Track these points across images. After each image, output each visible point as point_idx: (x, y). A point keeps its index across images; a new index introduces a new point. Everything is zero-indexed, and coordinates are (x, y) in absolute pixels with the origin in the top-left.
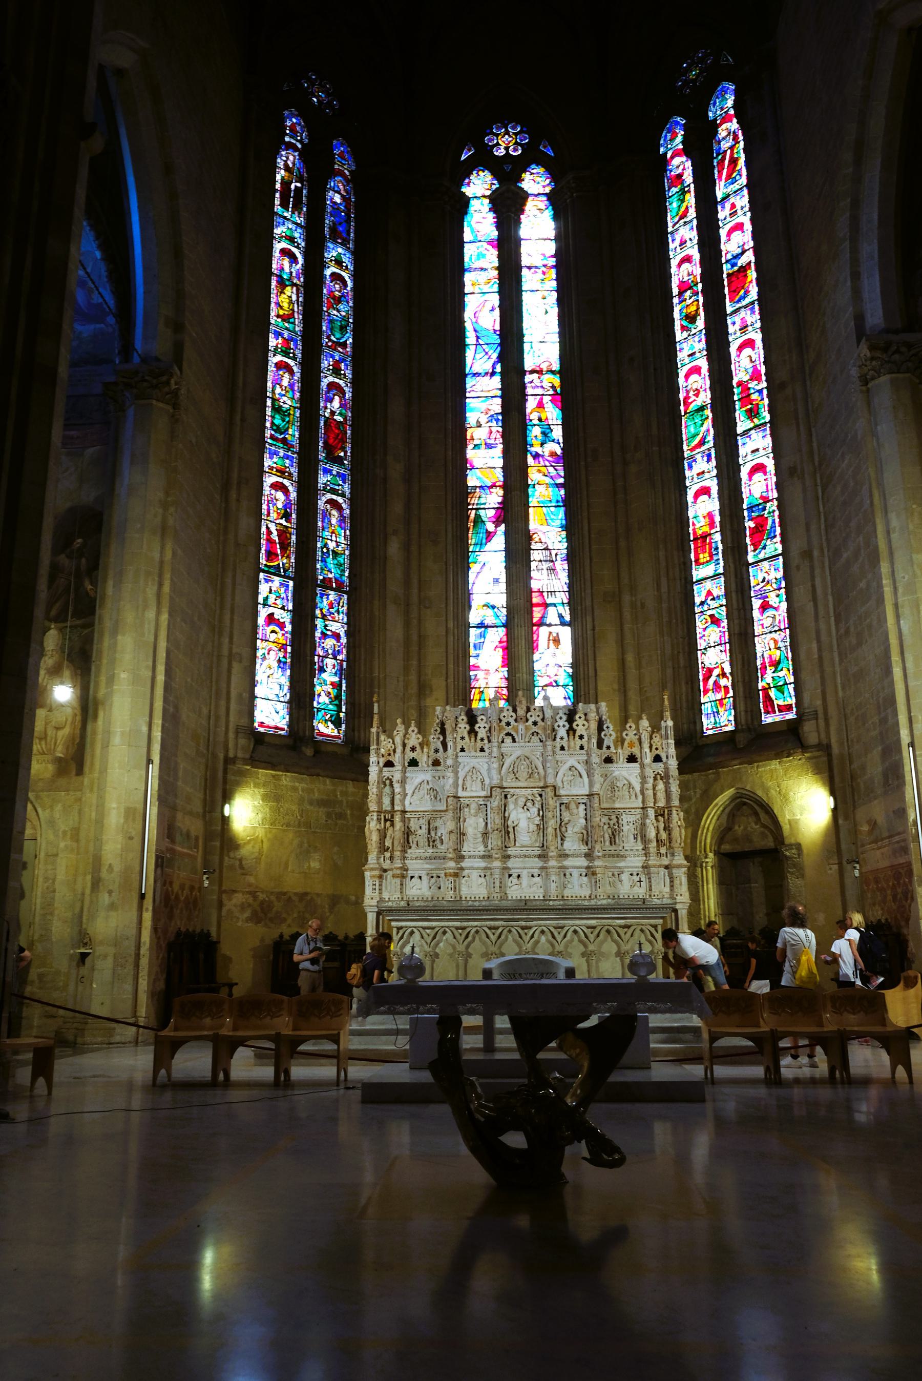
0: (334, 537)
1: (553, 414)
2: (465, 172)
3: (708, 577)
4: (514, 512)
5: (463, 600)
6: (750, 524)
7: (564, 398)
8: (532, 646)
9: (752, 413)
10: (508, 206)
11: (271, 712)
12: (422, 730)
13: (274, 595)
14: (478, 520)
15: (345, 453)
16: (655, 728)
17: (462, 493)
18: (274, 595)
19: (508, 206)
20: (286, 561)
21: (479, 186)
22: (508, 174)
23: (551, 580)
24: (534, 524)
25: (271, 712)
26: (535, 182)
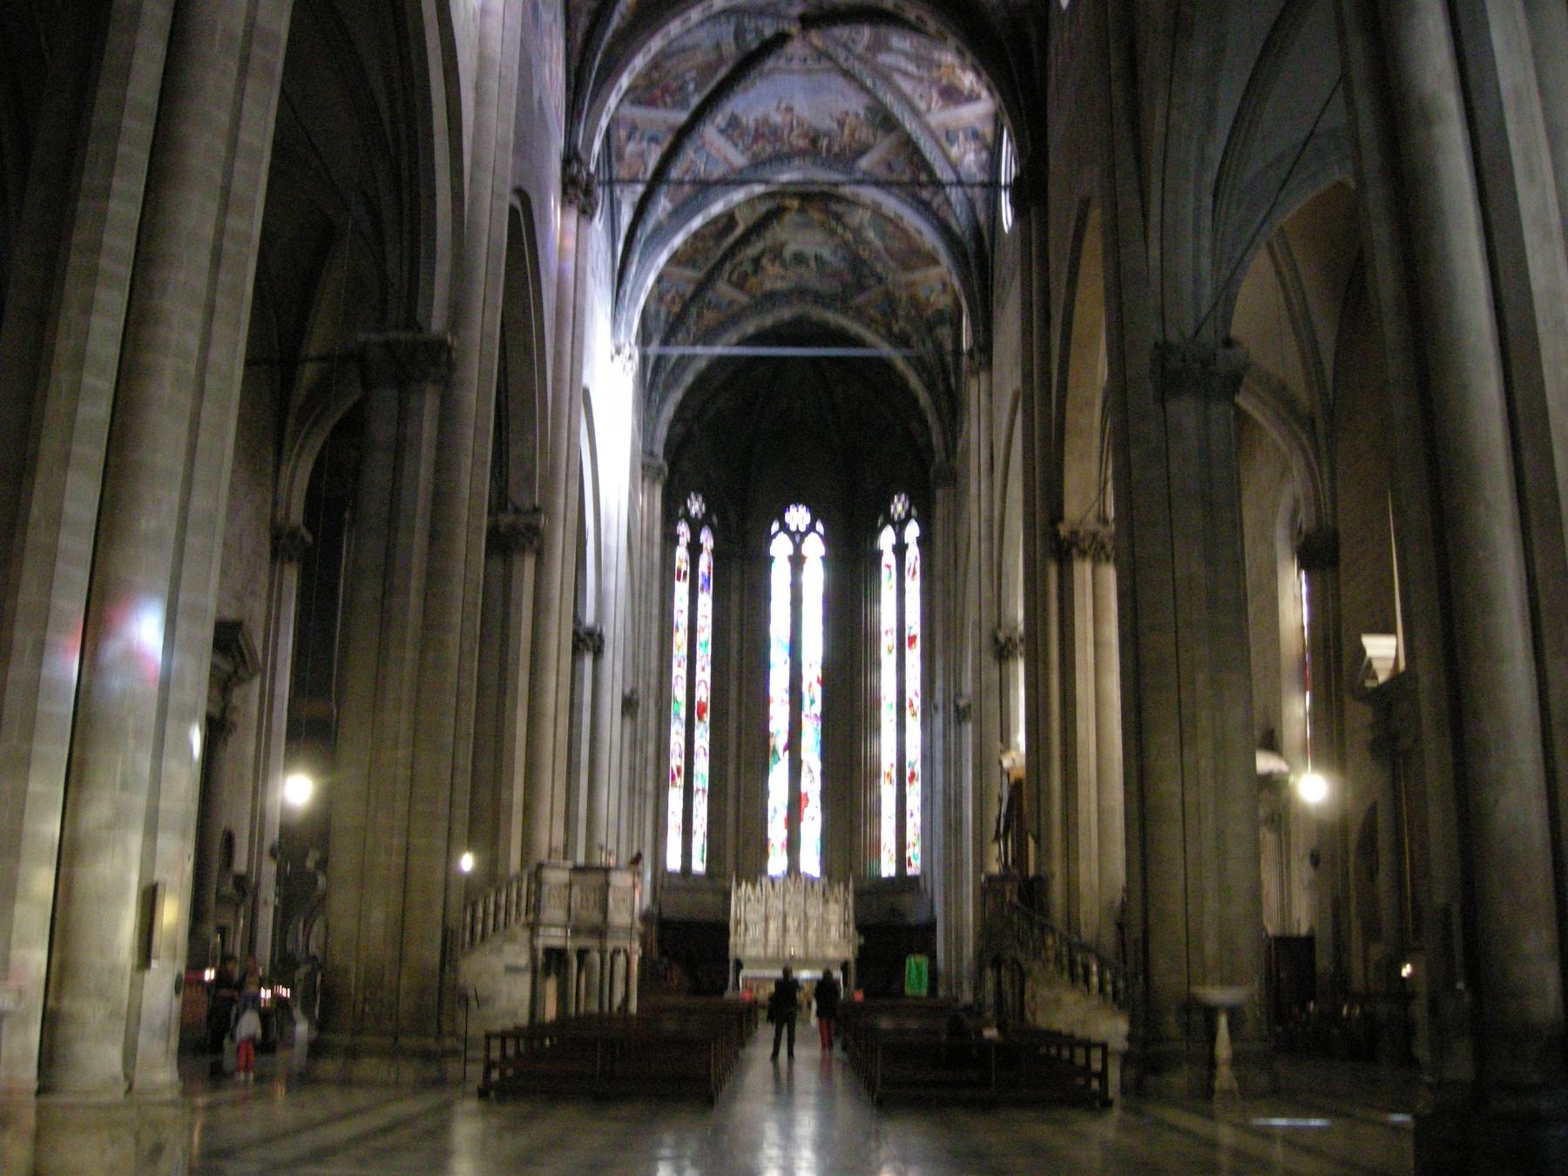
0: (702, 766)
1: (817, 691)
2: (770, 538)
3: (888, 793)
4: (794, 744)
5: (763, 794)
6: (908, 774)
7: (825, 682)
8: (799, 819)
9: (914, 714)
10: (797, 561)
11: (674, 862)
12: (754, 886)
13: (675, 797)
14: (775, 751)
15: (707, 717)
16: (846, 887)
17: (766, 735)
18: (675, 797)
19: (797, 561)
20: (680, 781)
21: (780, 548)
22: (798, 538)
23: (812, 785)
24: (804, 756)
25: (674, 862)
26: (814, 548)
